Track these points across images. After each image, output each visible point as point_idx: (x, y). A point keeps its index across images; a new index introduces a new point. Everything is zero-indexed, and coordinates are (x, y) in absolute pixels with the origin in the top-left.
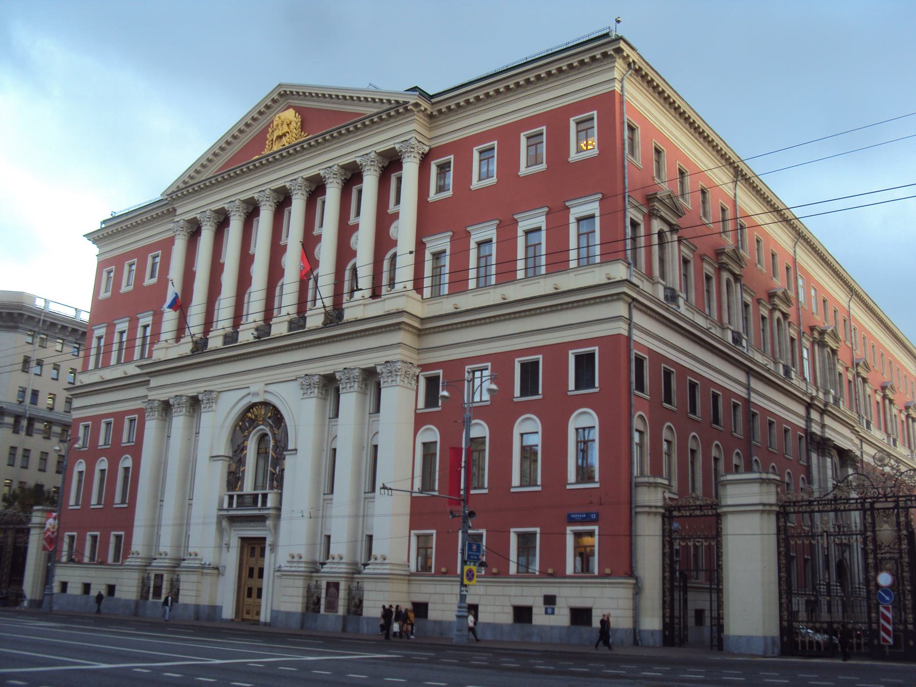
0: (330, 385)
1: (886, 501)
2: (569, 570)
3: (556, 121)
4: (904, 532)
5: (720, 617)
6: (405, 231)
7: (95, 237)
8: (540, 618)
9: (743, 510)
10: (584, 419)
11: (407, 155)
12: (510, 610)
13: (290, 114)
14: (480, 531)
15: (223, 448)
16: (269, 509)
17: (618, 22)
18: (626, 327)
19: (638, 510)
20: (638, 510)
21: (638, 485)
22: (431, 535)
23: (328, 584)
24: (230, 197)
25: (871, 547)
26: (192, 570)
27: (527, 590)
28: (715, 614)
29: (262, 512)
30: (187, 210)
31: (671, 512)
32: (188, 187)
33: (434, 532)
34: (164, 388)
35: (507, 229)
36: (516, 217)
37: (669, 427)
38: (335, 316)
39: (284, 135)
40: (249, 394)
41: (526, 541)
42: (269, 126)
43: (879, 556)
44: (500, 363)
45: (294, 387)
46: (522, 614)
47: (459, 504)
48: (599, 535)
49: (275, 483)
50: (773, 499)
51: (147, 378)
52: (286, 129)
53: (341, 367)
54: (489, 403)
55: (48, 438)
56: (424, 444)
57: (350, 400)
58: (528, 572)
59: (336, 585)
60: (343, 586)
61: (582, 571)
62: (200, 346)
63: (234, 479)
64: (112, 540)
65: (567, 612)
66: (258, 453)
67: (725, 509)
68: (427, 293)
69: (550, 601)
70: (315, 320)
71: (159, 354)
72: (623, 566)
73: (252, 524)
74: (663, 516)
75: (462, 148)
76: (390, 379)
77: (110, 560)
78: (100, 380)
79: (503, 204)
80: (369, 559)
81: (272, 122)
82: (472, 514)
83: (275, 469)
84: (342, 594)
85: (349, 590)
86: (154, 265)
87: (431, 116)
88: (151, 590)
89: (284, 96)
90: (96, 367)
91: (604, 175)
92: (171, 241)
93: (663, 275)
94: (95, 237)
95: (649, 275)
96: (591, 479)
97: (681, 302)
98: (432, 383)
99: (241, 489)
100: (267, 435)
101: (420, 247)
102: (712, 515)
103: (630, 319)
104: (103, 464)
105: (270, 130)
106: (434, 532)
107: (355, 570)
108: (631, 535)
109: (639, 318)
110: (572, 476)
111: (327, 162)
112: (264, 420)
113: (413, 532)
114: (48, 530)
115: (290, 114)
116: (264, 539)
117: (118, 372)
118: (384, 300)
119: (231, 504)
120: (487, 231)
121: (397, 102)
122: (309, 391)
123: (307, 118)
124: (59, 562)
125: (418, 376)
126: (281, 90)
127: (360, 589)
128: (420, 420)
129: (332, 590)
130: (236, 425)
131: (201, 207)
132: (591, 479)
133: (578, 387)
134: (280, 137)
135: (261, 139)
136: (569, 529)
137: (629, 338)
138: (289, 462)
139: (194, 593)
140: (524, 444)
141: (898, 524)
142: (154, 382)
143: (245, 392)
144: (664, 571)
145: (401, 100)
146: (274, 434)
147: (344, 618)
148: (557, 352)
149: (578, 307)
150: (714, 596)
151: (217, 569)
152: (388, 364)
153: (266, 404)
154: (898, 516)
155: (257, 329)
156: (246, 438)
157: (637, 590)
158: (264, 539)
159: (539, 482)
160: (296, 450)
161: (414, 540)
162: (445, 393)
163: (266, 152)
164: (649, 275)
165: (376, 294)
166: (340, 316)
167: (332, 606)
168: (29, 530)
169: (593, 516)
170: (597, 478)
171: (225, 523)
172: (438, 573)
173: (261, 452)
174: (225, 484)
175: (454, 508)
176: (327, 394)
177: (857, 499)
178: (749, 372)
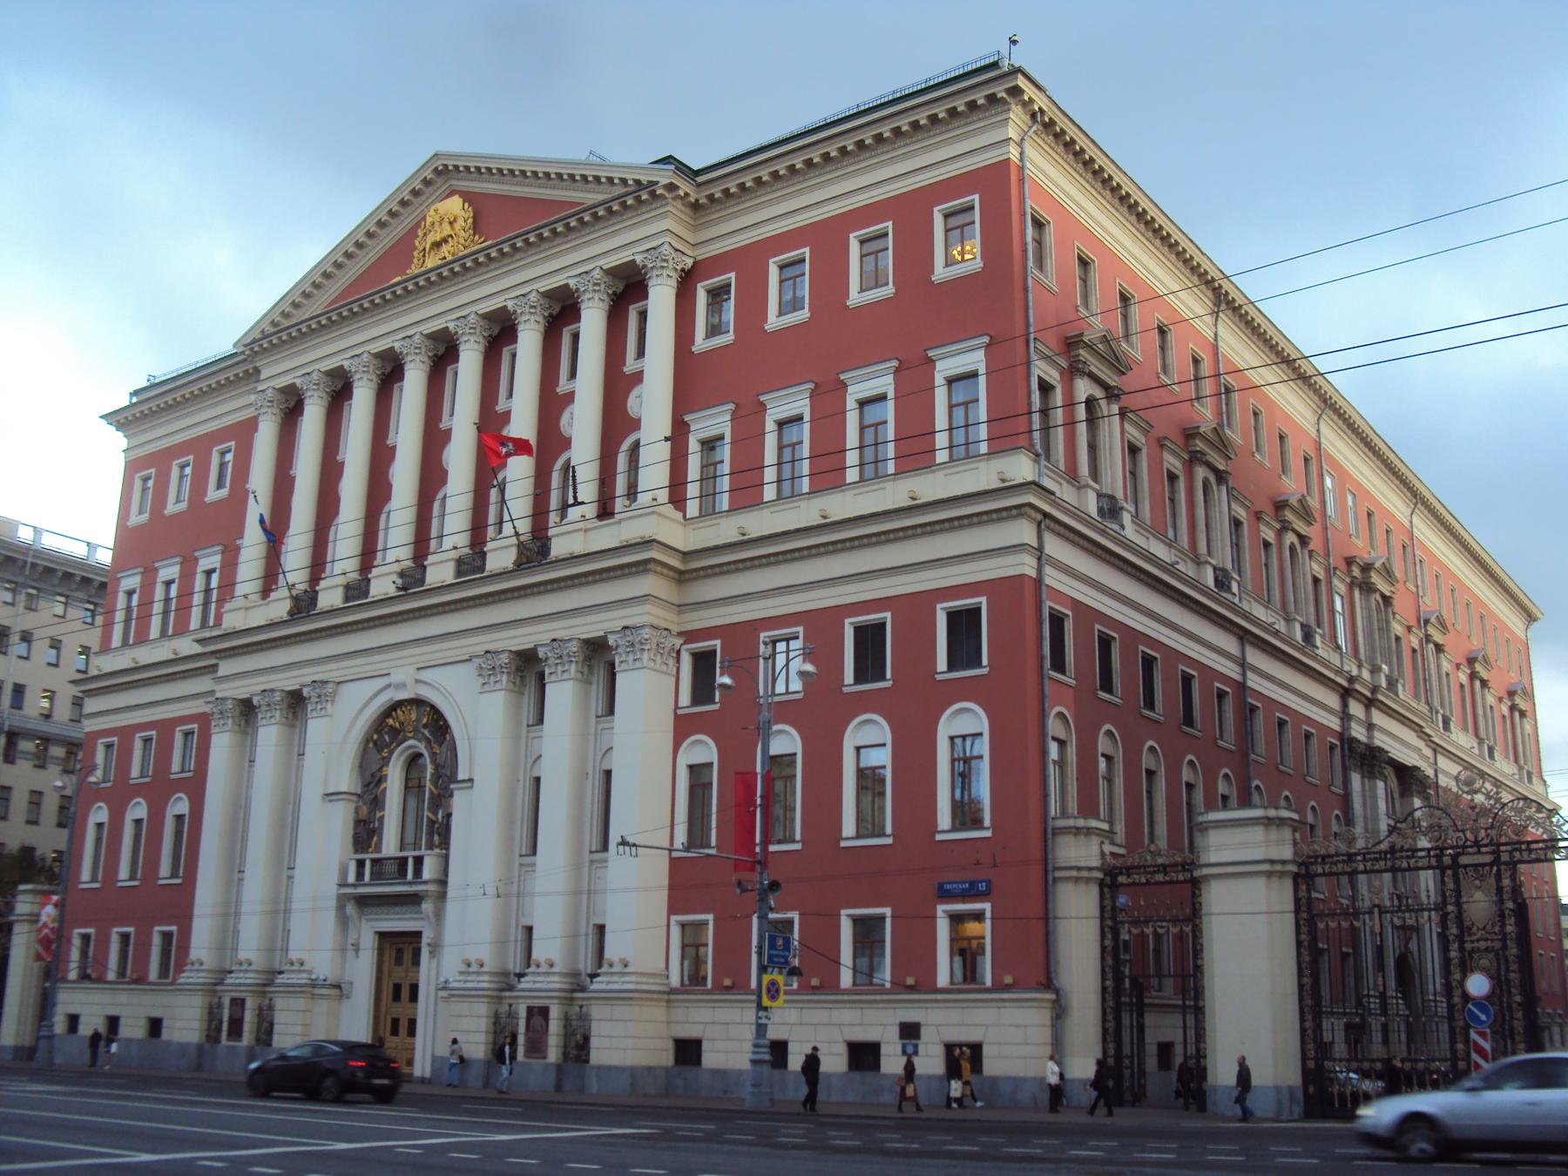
0: (528, 669)
1: (1479, 852)
2: (943, 979)
3: (910, 213)
4: (1510, 905)
5: (1200, 1055)
6: (653, 403)
7: (121, 420)
8: (892, 1063)
9: (1239, 871)
10: (964, 722)
11: (655, 272)
13: (454, 205)
14: (789, 915)
15: (346, 779)
16: (426, 882)
17: (1014, 42)
18: (1034, 562)
19: (1058, 874)
20: (1058, 874)
21: (1057, 832)
22: (706, 923)
23: (530, 1010)
24: (354, 347)
25: (1454, 930)
26: (294, 990)
27: (871, 1015)
28: (1191, 1050)
29: (414, 888)
30: (278, 372)
31: (1114, 877)
32: (280, 332)
33: (710, 917)
34: (244, 678)
35: (828, 397)
36: (762, 398)
37: (1109, 733)
38: (535, 550)
39: (445, 240)
40: (389, 686)
41: (867, 931)
42: (418, 225)
43: (1468, 946)
45: (468, 671)
46: (864, 1055)
47: (753, 869)
48: (992, 918)
49: (436, 838)
50: (1287, 852)
51: (214, 661)
52: (447, 230)
53: (546, 638)
54: (800, 696)
55: (42, 767)
56: (691, 767)
57: (562, 694)
58: (871, 984)
59: (544, 1012)
60: (555, 1013)
61: (965, 979)
62: (304, 604)
63: (365, 833)
64: (157, 941)
65: (939, 1051)
66: (406, 787)
67: (1205, 871)
68: (693, 508)
69: (910, 1031)
70: (501, 556)
71: (234, 620)
72: (1036, 972)
73: (397, 909)
74: (1102, 884)
75: (749, 260)
76: (631, 657)
77: (153, 974)
78: (132, 665)
79: (823, 354)
80: (600, 966)
81: (424, 218)
82: (774, 886)
83: (436, 814)
84: (555, 1026)
85: (567, 1020)
86: (222, 466)
87: (696, 206)
88: (225, 1026)
89: (443, 174)
90: (125, 643)
91: (991, 303)
92: (251, 426)
93: (1095, 473)
94: (121, 420)
95: (1072, 474)
96: (977, 823)
97: (1126, 518)
98: (704, 664)
99: (378, 849)
100: (421, 755)
101: (679, 432)
102: (1185, 882)
103: (1040, 549)
104: (138, 810)
105: (420, 233)
106: (710, 917)
107: (577, 985)
108: (1047, 917)
109: (1055, 547)
110: (944, 819)
111: (520, 285)
112: (416, 730)
113: (674, 918)
114: (45, 925)
115: (454, 205)
116: (418, 934)
117: (162, 652)
118: (620, 522)
119: (360, 874)
120: (794, 402)
121: (638, 182)
122: (492, 679)
123: (483, 212)
124: (64, 979)
125: (678, 652)
126: (439, 164)
127: (585, 1018)
128: (684, 727)
129: (537, 1020)
130: (367, 740)
131: (304, 365)
132: (977, 823)
133: (952, 666)
134: (437, 245)
135: (403, 249)
136: (941, 909)
137: (1038, 581)
138: (460, 802)
139: (298, 1030)
140: (862, 765)
141: (1500, 890)
142: (226, 668)
144: (1104, 979)
145: (644, 179)
146: (433, 755)
147: (559, 1067)
148: (915, 607)
149: (870, 545)
150: (1190, 1020)
151: (338, 987)
152: (628, 632)
153: (418, 702)
154: (1498, 877)
155: (402, 574)
156: (386, 761)
157: (1059, 1012)
158: (418, 934)
159: (889, 830)
160: (471, 780)
161: (676, 933)
162: (727, 680)
163: (414, 270)
164: (1072, 474)
165: (605, 511)
166: (544, 550)
167: (536, 1047)
168: (10, 926)
169: (982, 887)
170: (987, 822)
171: (351, 909)
172: (719, 988)
173: (412, 785)
174: (350, 840)
175: (744, 875)
176: (523, 684)
177: (1429, 850)
178: (1244, 636)
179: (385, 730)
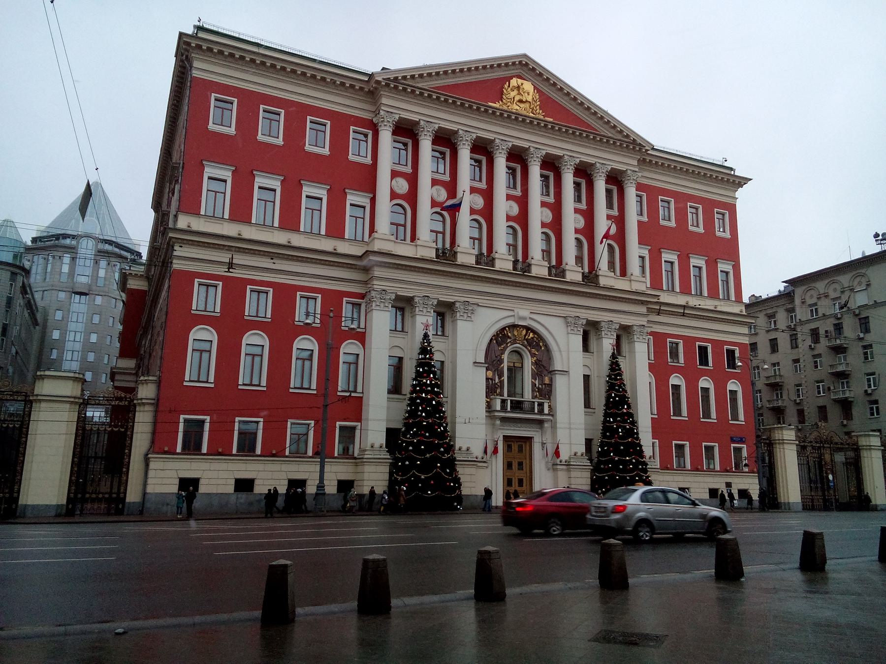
13: (528, 86)
14: (337, 426)
27: (717, 479)
50: (78, 393)
69: (729, 485)
89: (525, 66)
126: (524, 61)
143: (511, 313)
153: (528, 329)
162: (740, 364)
179: (501, 337)
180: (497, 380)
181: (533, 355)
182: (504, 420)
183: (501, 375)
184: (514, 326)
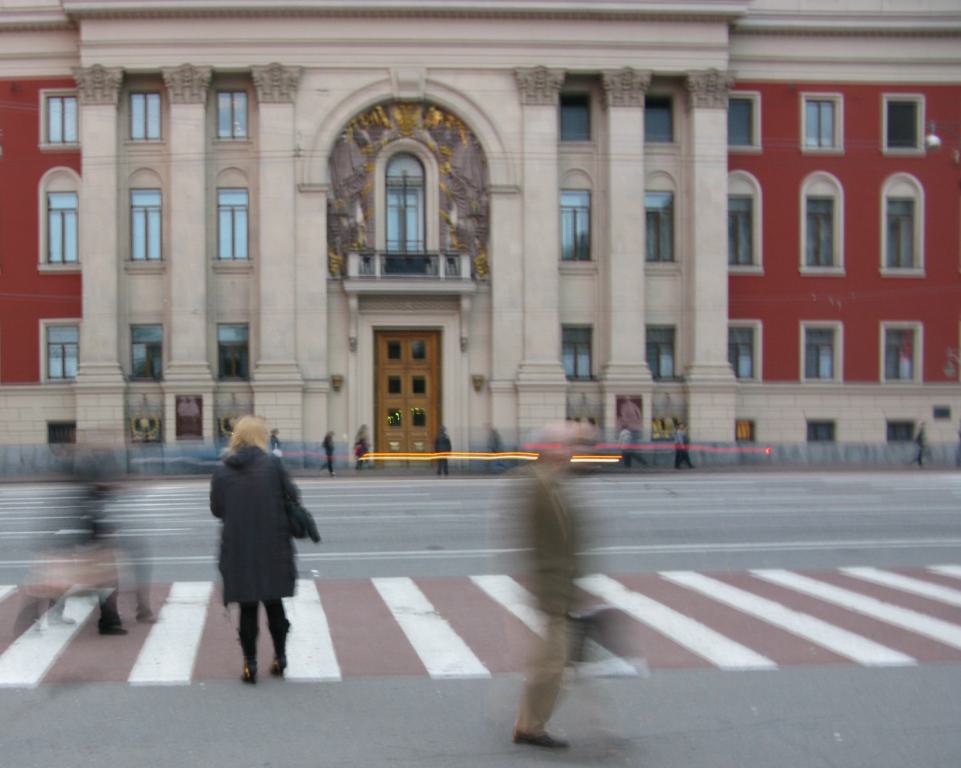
12: (803, 427)
23: (620, 401)
44: (860, 98)
45: (503, 85)
57: (625, 123)
66: (387, 185)
80: (524, 358)
83: (448, 213)
84: (647, 413)
129: (630, 407)
153: (426, 105)
156: (371, 158)
179: (369, 122)
180: (359, 216)
181: (441, 158)
182: (365, 298)
183: (367, 207)
184: (388, 105)
